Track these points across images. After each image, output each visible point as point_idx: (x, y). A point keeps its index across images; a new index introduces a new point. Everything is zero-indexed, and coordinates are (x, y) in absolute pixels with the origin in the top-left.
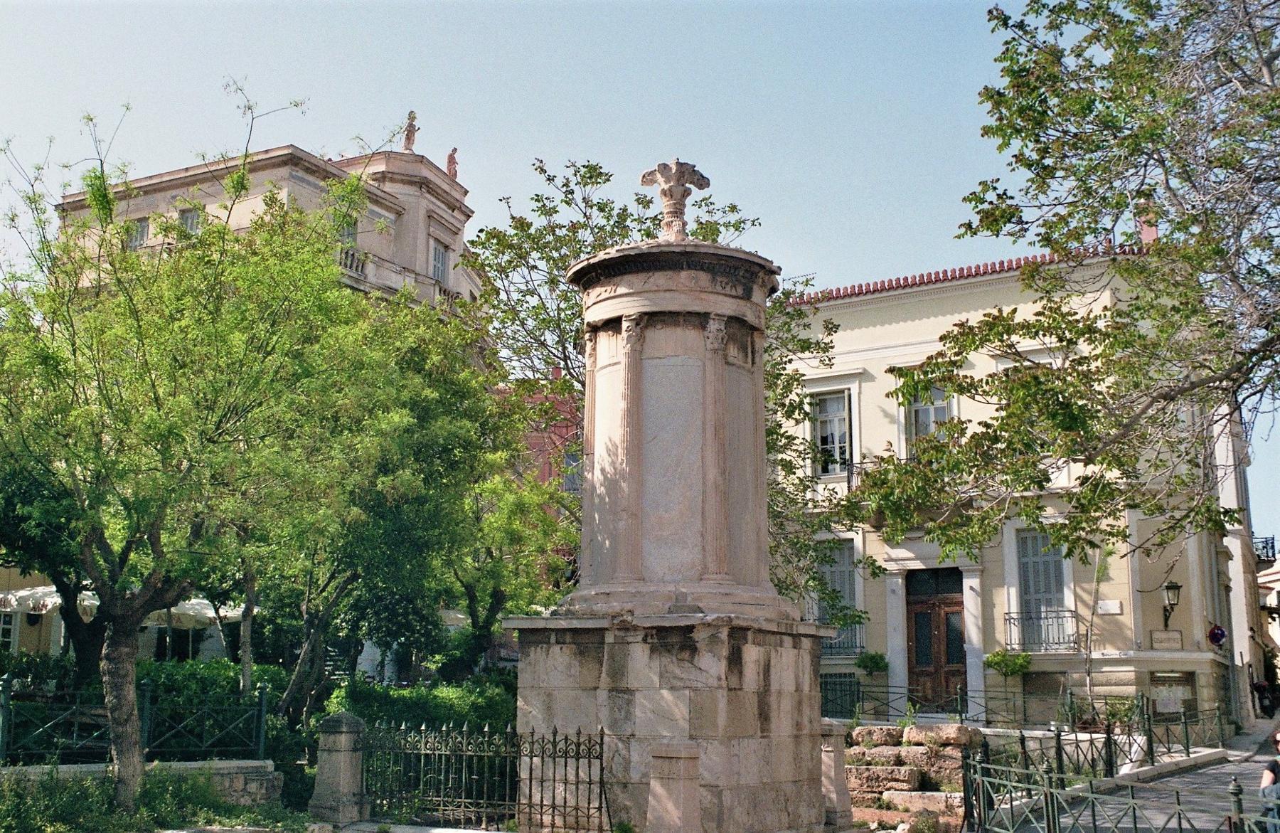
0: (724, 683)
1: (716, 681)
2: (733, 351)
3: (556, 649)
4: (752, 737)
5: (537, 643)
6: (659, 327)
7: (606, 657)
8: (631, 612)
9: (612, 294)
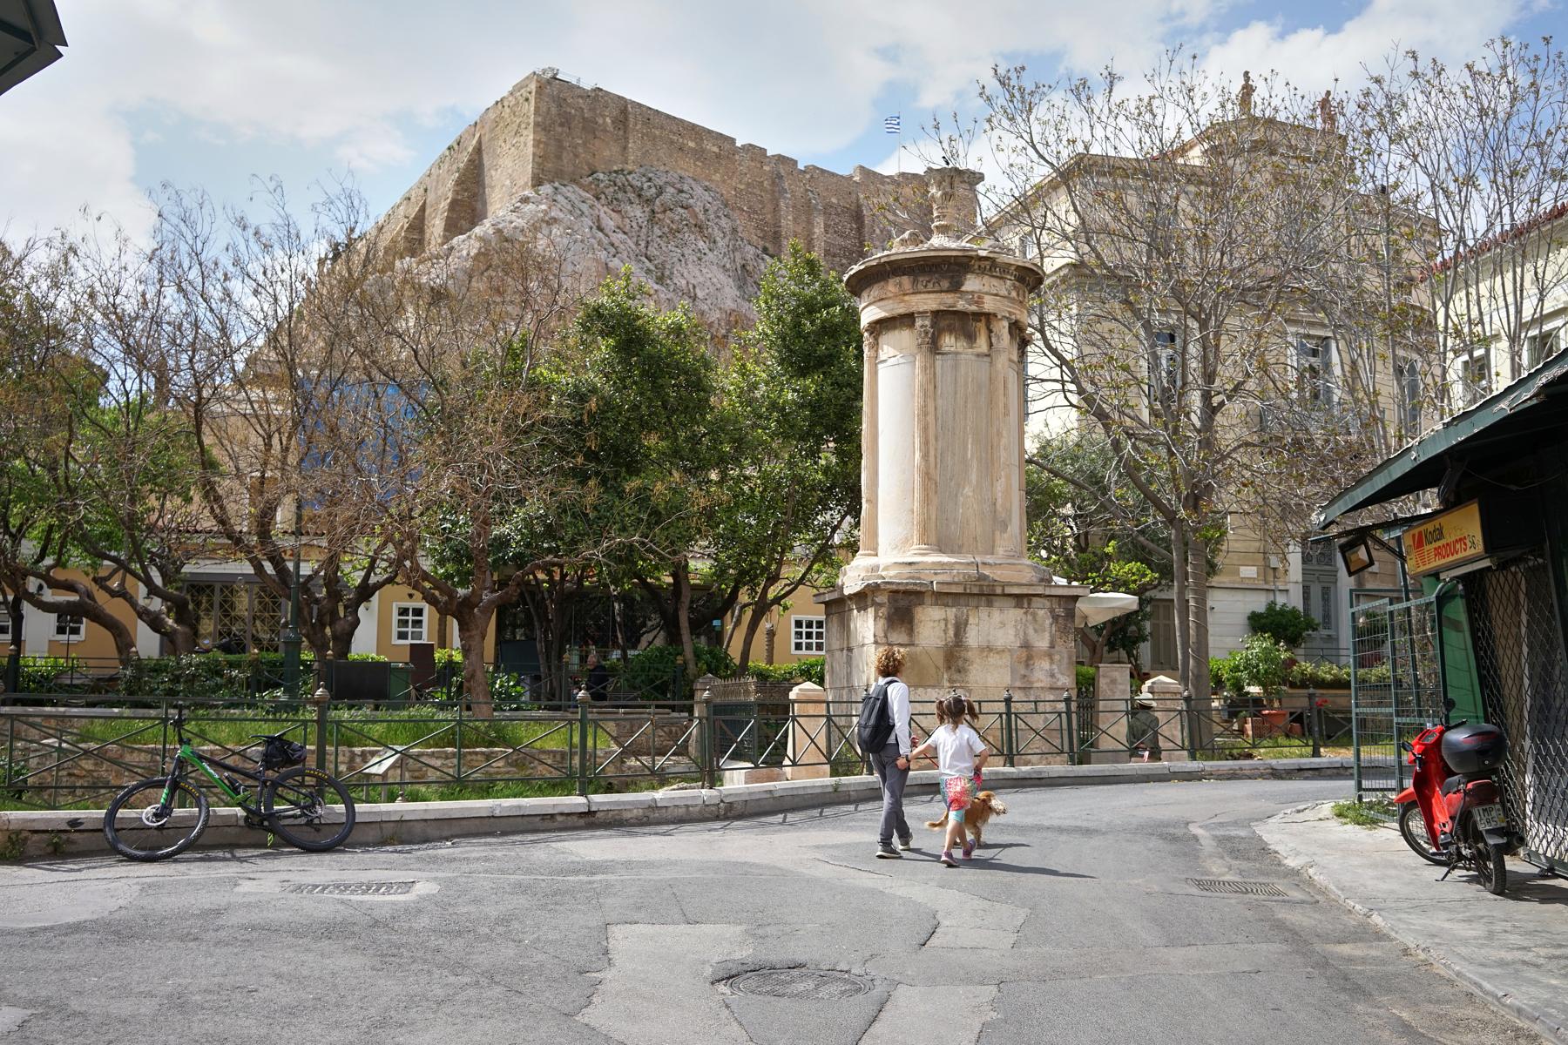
0: (884, 640)
2: (948, 342)
4: (933, 687)
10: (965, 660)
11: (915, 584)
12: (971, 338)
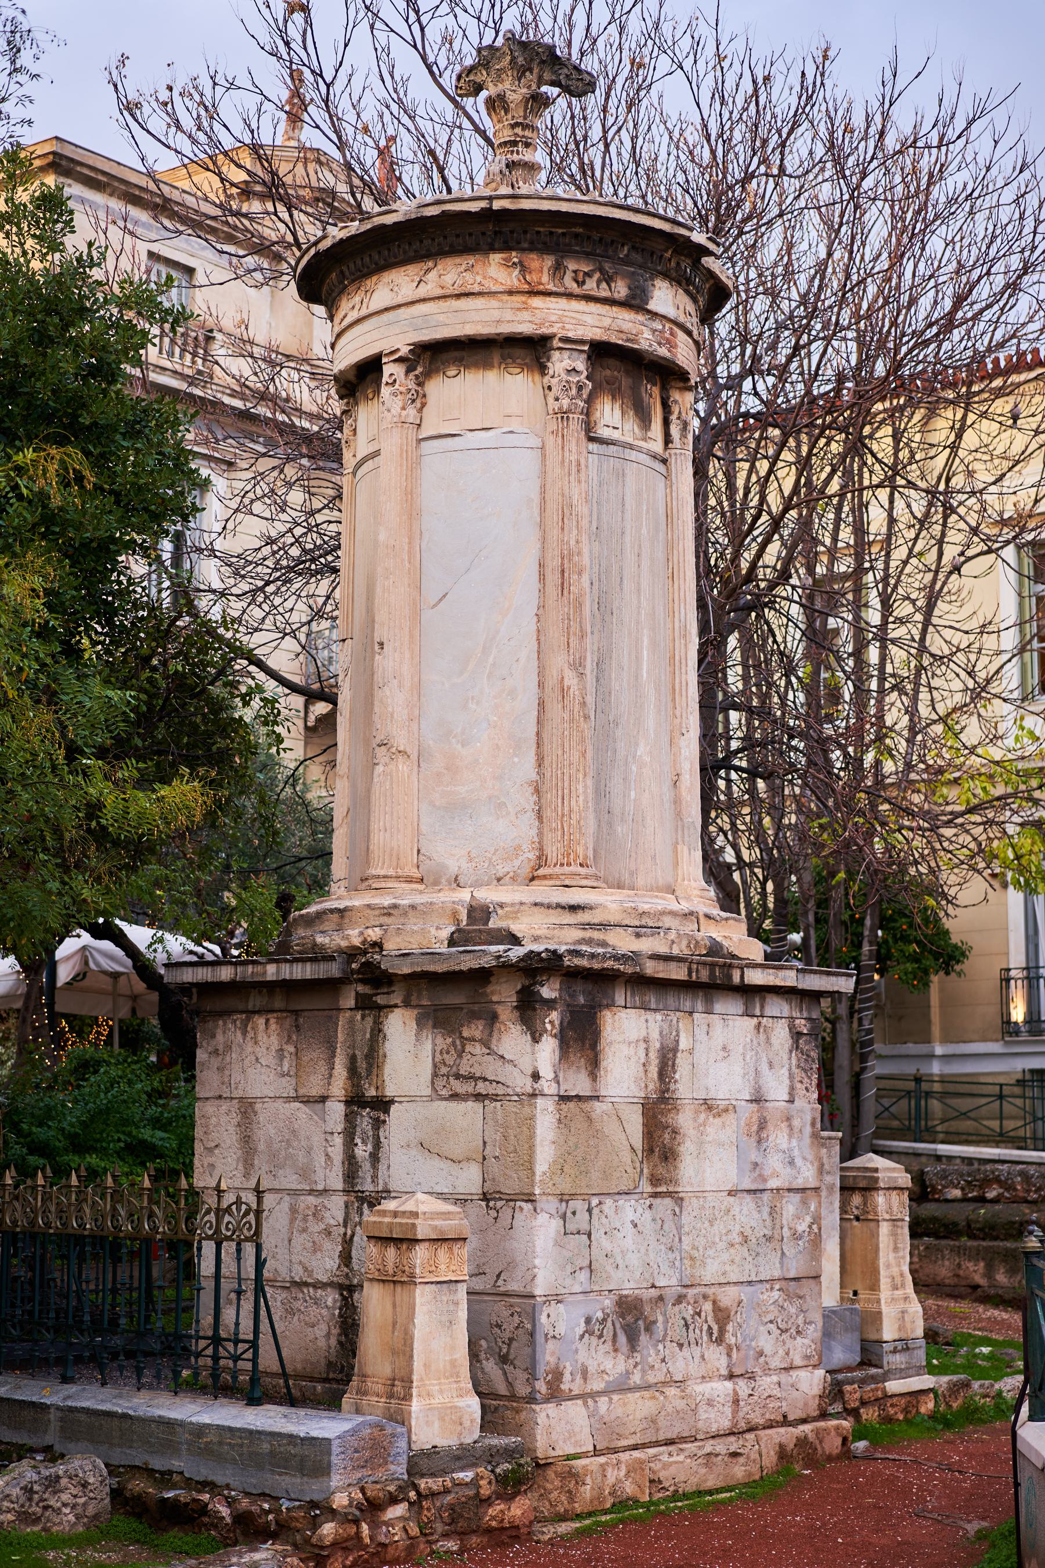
1: (529, 1081)
3: (261, 1021)
5: (225, 1013)
6: (452, 372)
7: (341, 1037)
8: (378, 945)
9: (364, 312)
10: (675, 1132)
11: (616, 958)
12: (644, 419)
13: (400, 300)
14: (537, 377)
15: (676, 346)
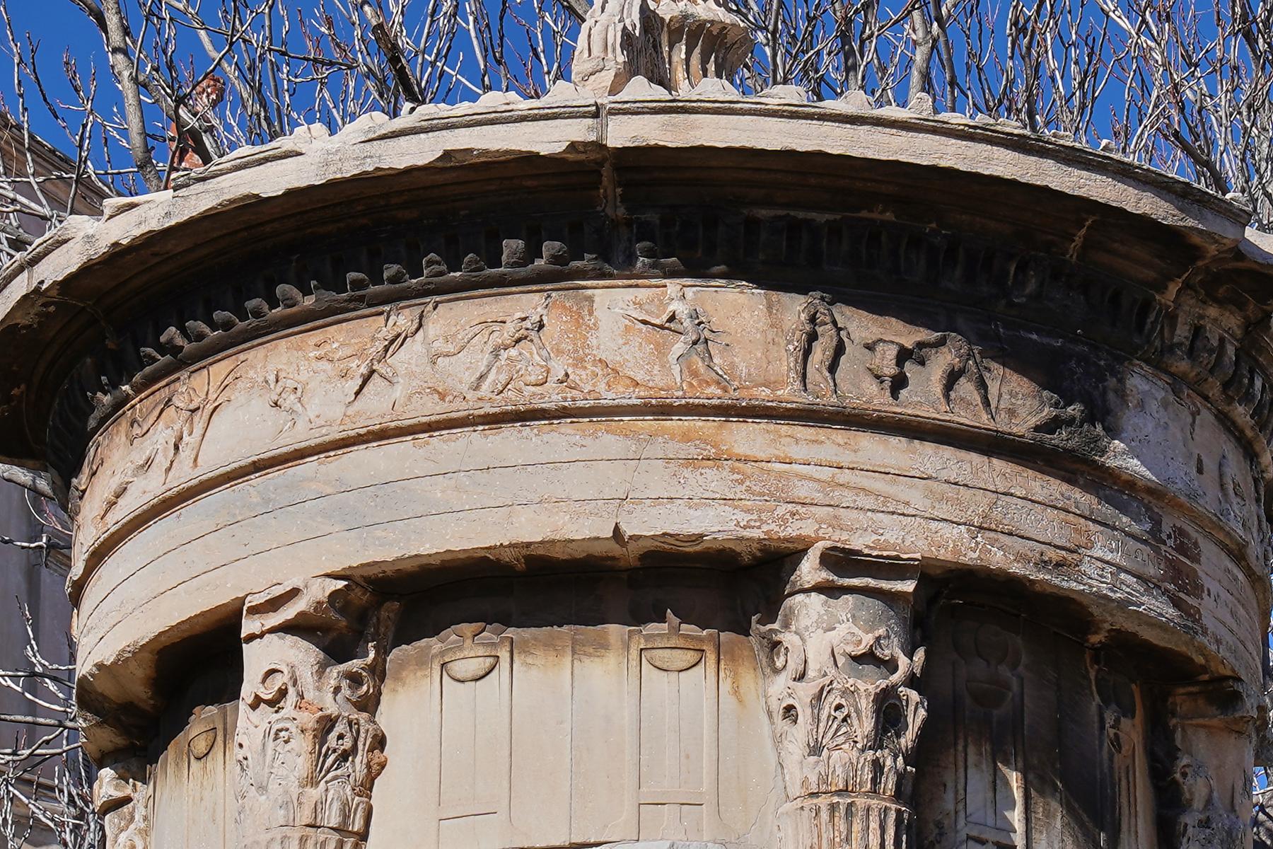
9: (184, 475)
13: (300, 436)
14: (748, 680)
15: (1197, 589)
